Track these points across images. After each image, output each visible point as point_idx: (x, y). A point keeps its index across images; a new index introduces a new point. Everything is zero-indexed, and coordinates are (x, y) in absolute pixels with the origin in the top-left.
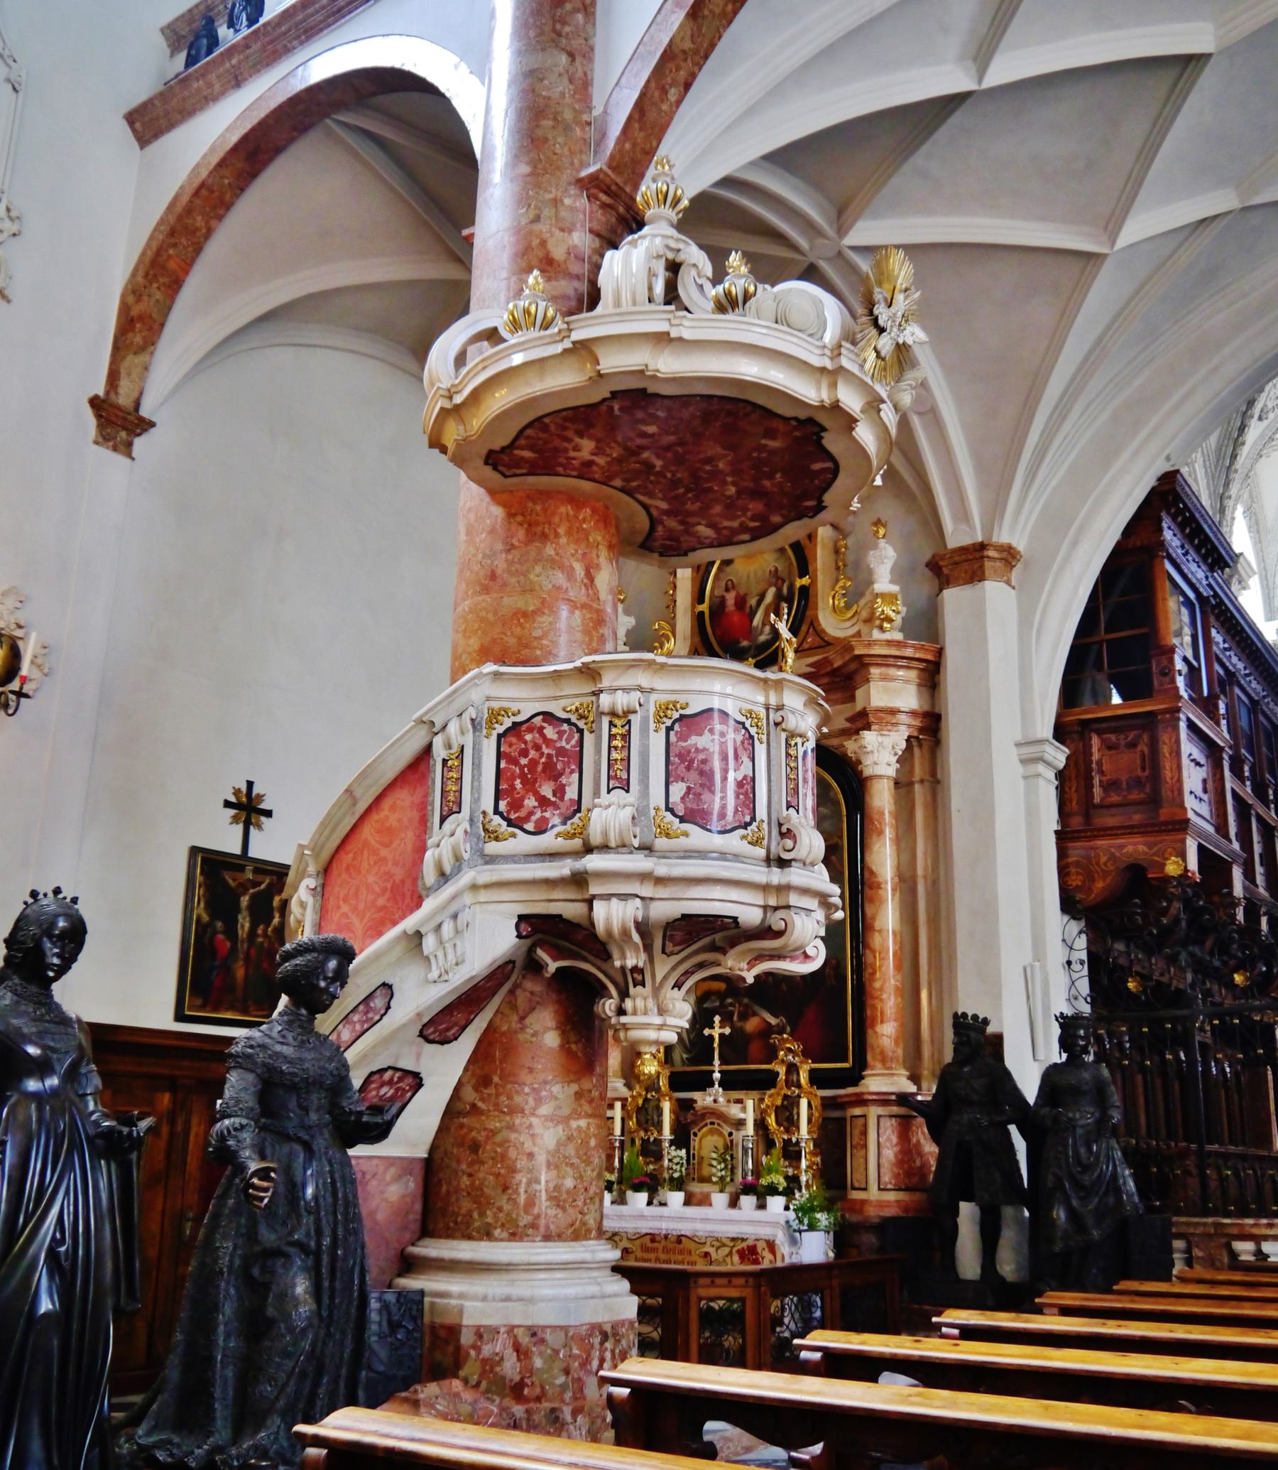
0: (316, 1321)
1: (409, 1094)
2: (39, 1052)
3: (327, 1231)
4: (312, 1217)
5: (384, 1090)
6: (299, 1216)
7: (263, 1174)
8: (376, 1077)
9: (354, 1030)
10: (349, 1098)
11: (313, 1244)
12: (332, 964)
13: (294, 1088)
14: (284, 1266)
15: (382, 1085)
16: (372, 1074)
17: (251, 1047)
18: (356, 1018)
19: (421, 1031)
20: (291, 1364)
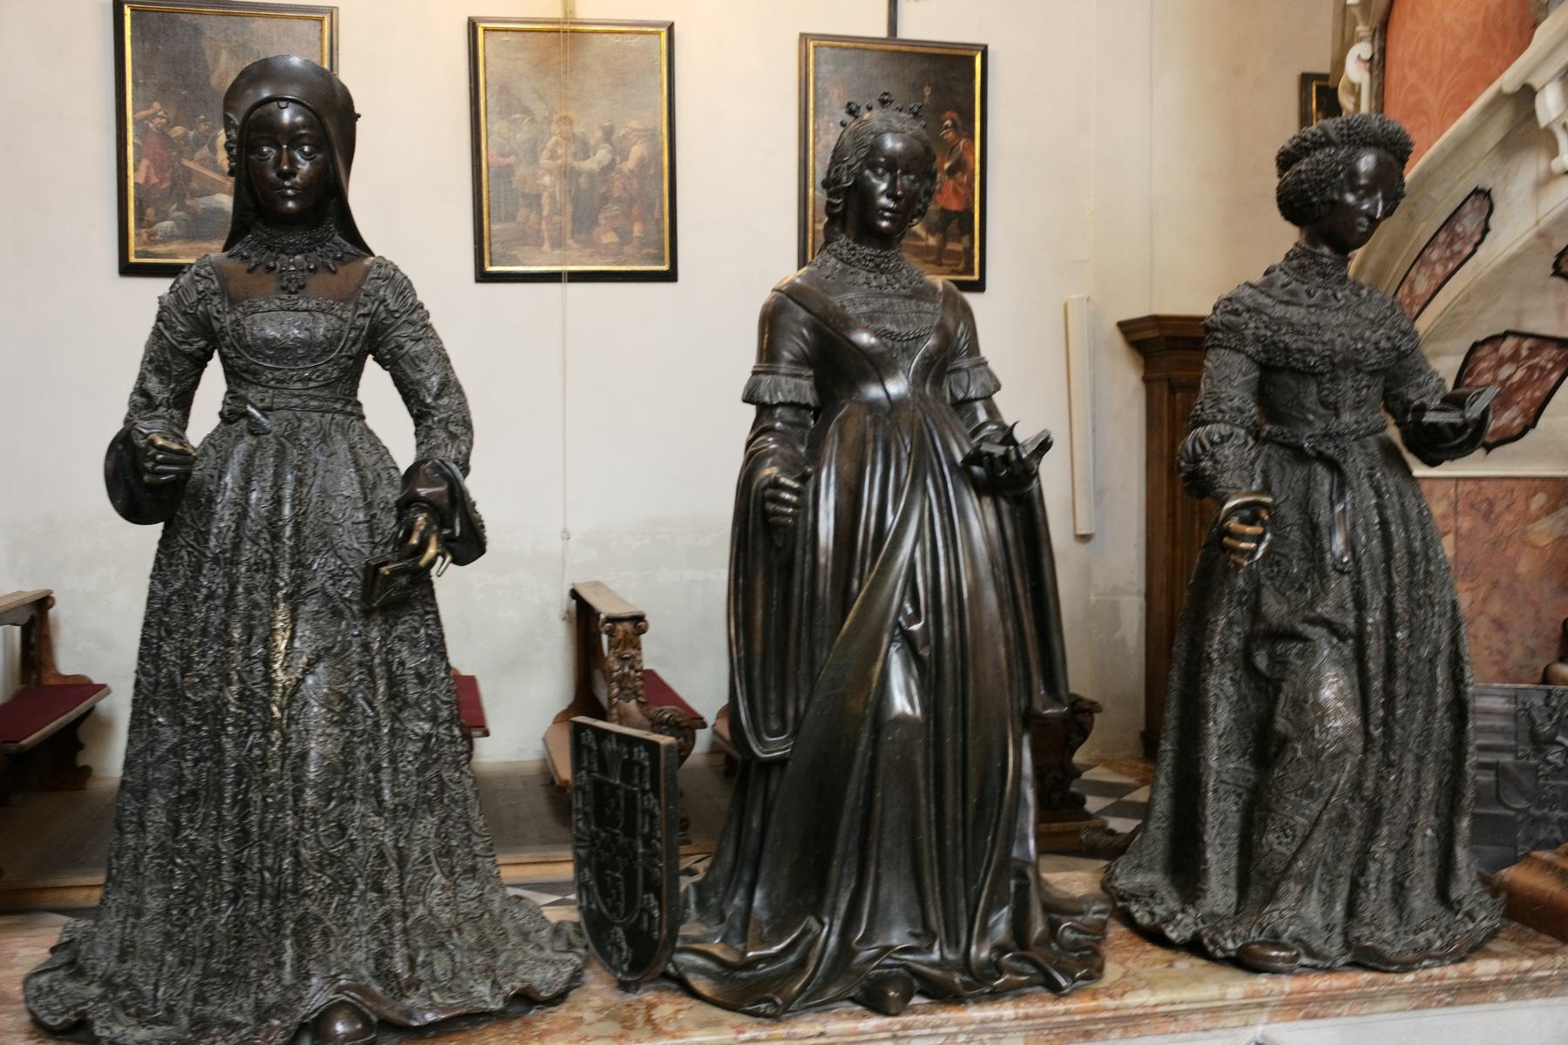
0: (1357, 744)
1: (1555, 376)
2: (873, 340)
3: (1375, 600)
4: (1346, 578)
5: (1505, 371)
6: (1323, 576)
7: (1251, 513)
8: (1486, 350)
9: (1432, 276)
10: (1419, 386)
11: (1350, 622)
12: (1366, 162)
13: (1308, 373)
14: (1301, 655)
15: (1501, 363)
16: (1475, 347)
17: (1236, 313)
18: (1435, 255)
19: (1557, 266)
20: (1316, 807)
